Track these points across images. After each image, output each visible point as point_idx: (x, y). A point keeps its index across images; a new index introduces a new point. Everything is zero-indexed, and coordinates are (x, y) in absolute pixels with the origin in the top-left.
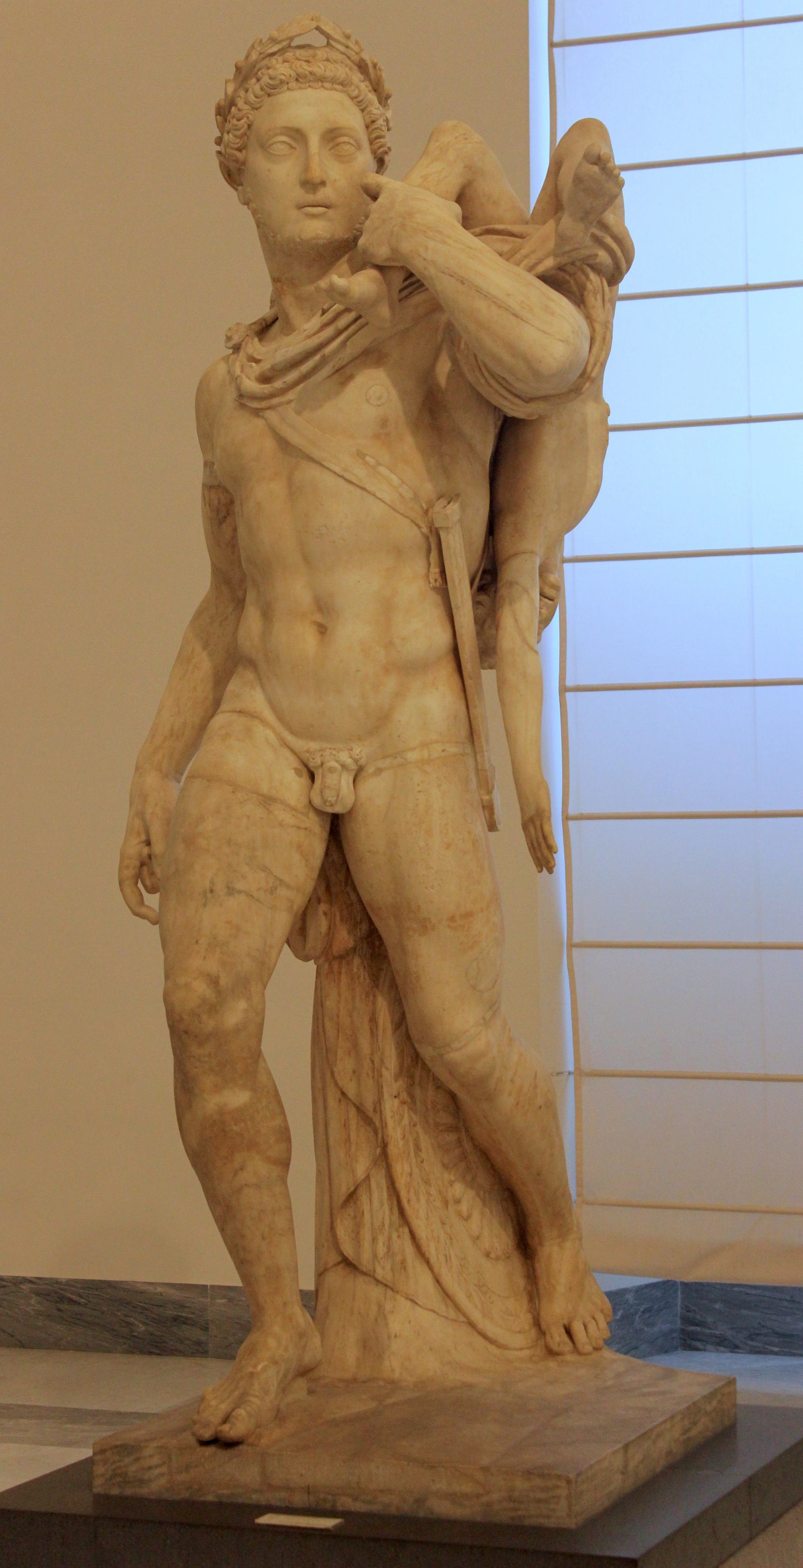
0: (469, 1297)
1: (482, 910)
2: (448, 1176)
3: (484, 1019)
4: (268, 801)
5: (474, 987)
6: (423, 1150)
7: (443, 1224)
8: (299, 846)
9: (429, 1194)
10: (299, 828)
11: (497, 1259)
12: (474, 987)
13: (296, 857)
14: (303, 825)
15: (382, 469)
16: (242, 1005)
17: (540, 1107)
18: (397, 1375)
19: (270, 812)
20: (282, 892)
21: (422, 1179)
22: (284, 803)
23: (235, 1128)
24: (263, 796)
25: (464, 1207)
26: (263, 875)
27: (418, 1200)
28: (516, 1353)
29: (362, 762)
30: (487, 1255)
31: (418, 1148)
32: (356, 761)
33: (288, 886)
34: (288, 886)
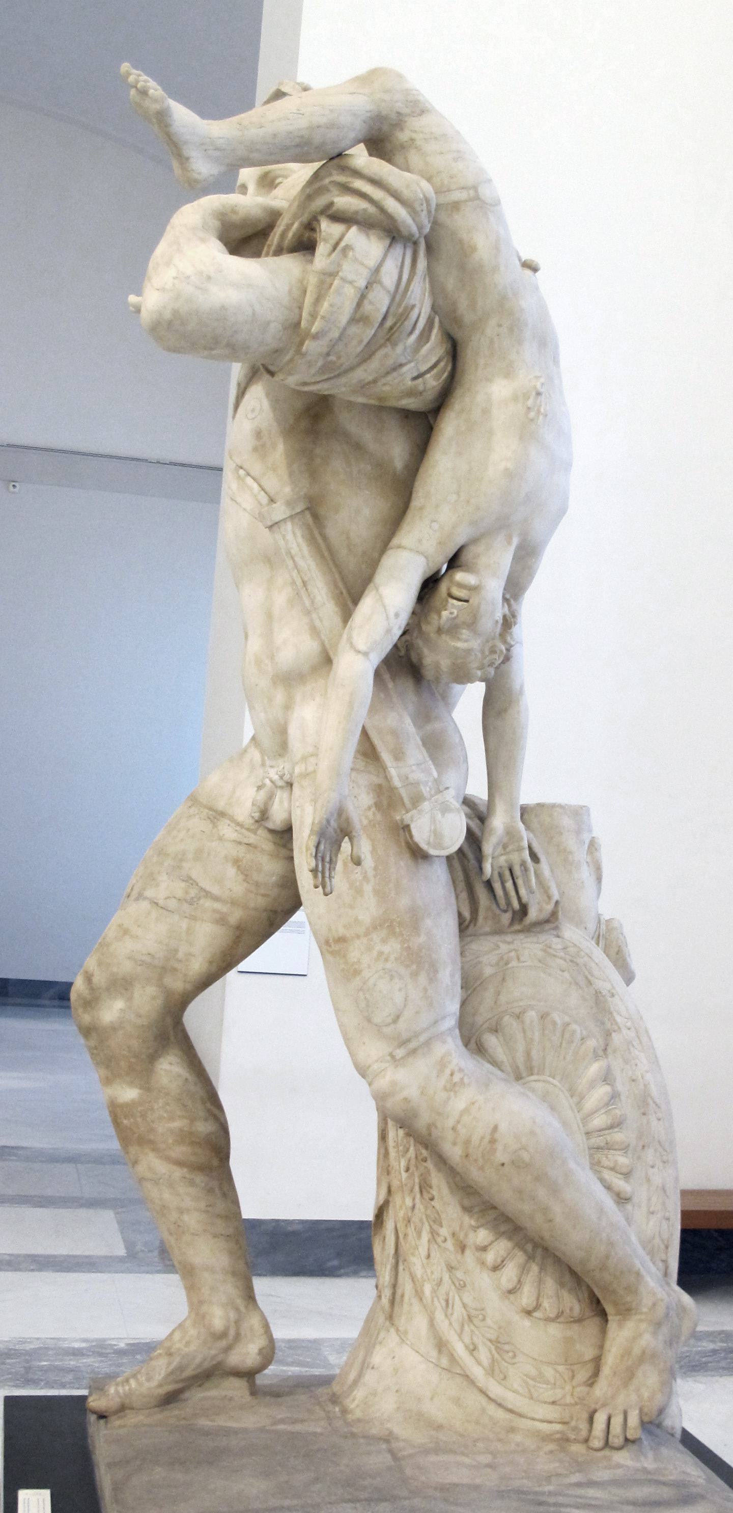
0: (473, 1350)
1: (358, 937)
2: (469, 1221)
3: (392, 1056)
4: (217, 815)
5: (369, 1020)
6: (434, 1187)
7: (451, 1268)
8: (237, 862)
9: (434, 1234)
10: (240, 843)
11: (548, 1320)
12: (369, 1020)
13: (231, 872)
14: (246, 841)
15: (249, 480)
16: (119, 1004)
17: (503, 1165)
18: (352, 1406)
19: (215, 826)
20: (208, 903)
21: (427, 1216)
22: (232, 820)
23: (125, 1122)
24: (216, 811)
25: (490, 1257)
26: (183, 885)
27: (419, 1235)
28: (537, 1424)
29: (287, 777)
30: (529, 1313)
31: (425, 1186)
32: (281, 777)
33: (216, 899)
34: (216, 899)
